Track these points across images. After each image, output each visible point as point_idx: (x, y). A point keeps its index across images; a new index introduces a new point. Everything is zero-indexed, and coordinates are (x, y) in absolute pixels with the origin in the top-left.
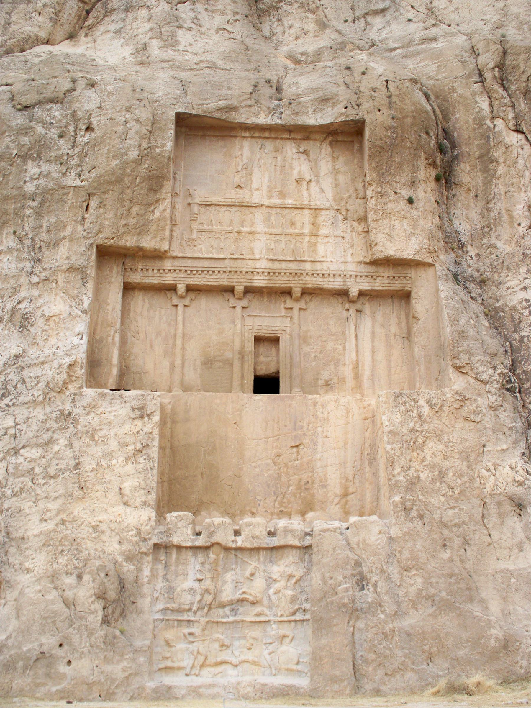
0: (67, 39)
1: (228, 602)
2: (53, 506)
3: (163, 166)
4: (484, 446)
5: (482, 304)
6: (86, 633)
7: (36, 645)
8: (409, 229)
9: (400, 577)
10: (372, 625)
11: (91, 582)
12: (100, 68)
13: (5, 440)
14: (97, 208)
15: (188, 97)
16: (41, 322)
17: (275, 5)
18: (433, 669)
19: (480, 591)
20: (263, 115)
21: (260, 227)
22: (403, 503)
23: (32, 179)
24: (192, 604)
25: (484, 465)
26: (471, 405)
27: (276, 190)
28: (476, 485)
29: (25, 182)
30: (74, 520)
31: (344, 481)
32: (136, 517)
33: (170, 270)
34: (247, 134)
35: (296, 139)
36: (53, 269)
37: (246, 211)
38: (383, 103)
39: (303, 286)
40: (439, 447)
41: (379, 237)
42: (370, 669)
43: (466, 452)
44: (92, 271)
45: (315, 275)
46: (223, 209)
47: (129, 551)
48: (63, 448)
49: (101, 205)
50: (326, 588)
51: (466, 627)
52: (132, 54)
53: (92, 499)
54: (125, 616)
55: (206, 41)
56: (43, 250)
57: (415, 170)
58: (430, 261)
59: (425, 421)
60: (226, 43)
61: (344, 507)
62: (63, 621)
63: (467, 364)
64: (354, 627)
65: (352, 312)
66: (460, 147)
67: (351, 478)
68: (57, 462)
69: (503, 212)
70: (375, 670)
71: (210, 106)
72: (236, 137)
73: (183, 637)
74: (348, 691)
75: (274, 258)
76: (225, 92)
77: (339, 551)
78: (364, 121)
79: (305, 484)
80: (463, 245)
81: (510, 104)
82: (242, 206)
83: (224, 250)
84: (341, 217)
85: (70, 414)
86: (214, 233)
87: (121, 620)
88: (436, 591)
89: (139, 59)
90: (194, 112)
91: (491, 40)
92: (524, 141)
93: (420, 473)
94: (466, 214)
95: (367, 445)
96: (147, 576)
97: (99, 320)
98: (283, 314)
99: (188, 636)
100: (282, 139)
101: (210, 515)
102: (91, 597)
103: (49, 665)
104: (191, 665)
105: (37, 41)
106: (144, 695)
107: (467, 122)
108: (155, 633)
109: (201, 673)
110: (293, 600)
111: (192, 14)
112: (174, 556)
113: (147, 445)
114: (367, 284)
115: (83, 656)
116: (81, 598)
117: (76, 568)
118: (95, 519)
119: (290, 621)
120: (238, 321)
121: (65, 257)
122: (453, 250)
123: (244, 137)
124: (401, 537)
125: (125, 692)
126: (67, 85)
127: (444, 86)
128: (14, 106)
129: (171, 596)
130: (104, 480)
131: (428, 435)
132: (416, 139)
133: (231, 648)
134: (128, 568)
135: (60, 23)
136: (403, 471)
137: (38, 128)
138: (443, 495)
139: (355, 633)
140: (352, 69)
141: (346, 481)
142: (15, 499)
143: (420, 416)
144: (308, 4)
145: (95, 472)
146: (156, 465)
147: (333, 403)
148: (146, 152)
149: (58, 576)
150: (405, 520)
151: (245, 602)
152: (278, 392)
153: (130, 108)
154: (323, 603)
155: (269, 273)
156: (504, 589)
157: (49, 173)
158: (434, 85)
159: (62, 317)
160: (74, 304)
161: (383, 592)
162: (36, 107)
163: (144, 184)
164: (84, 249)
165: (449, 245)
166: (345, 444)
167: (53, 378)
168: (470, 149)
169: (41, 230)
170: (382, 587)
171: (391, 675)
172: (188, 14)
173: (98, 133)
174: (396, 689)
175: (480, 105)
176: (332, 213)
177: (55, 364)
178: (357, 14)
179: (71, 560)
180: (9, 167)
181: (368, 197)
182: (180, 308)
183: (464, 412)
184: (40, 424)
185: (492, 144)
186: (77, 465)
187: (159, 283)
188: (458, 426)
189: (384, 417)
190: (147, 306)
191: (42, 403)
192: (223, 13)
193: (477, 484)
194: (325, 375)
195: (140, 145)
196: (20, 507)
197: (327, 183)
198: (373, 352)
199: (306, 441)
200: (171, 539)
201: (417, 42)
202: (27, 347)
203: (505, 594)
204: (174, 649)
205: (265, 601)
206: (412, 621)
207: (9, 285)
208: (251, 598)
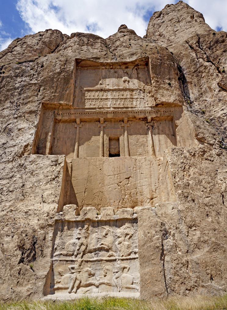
2: (8, 204)
3: (70, 74)
6: (9, 268)
24: (74, 251)
29: (16, 84)
32: (48, 207)
33: (73, 114)
34: (104, 68)
38: (155, 52)
41: (159, 96)
42: (177, 286)
48: (18, 179)
56: (20, 106)
67: (154, 190)
68: (14, 185)
73: (68, 270)
77: (152, 219)
79: (133, 194)
84: (142, 92)
85: (23, 164)
92: (211, 64)
93: (189, 181)
96: (51, 237)
115: (4, 282)
116: (10, 248)
118: (27, 209)
119: (127, 259)
129: (63, 247)
131: (190, 165)
145: (31, 189)
146: (61, 185)
149: (2, 237)
150: (186, 202)
154: (145, 247)
157: (25, 80)
164: (37, 104)
166: (151, 176)
169: (21, 99)
177: (20, 146)
179: (10, 229)
182: (78, 128)
183: (205, 156)
191: (12, 161)
192: (97, 49)
195: (61, 68)
198: (159, 141)
200: (65, 218)
204: (63, 277)
205: (114, 248)
206: (198, 256)
208: (106, 247)
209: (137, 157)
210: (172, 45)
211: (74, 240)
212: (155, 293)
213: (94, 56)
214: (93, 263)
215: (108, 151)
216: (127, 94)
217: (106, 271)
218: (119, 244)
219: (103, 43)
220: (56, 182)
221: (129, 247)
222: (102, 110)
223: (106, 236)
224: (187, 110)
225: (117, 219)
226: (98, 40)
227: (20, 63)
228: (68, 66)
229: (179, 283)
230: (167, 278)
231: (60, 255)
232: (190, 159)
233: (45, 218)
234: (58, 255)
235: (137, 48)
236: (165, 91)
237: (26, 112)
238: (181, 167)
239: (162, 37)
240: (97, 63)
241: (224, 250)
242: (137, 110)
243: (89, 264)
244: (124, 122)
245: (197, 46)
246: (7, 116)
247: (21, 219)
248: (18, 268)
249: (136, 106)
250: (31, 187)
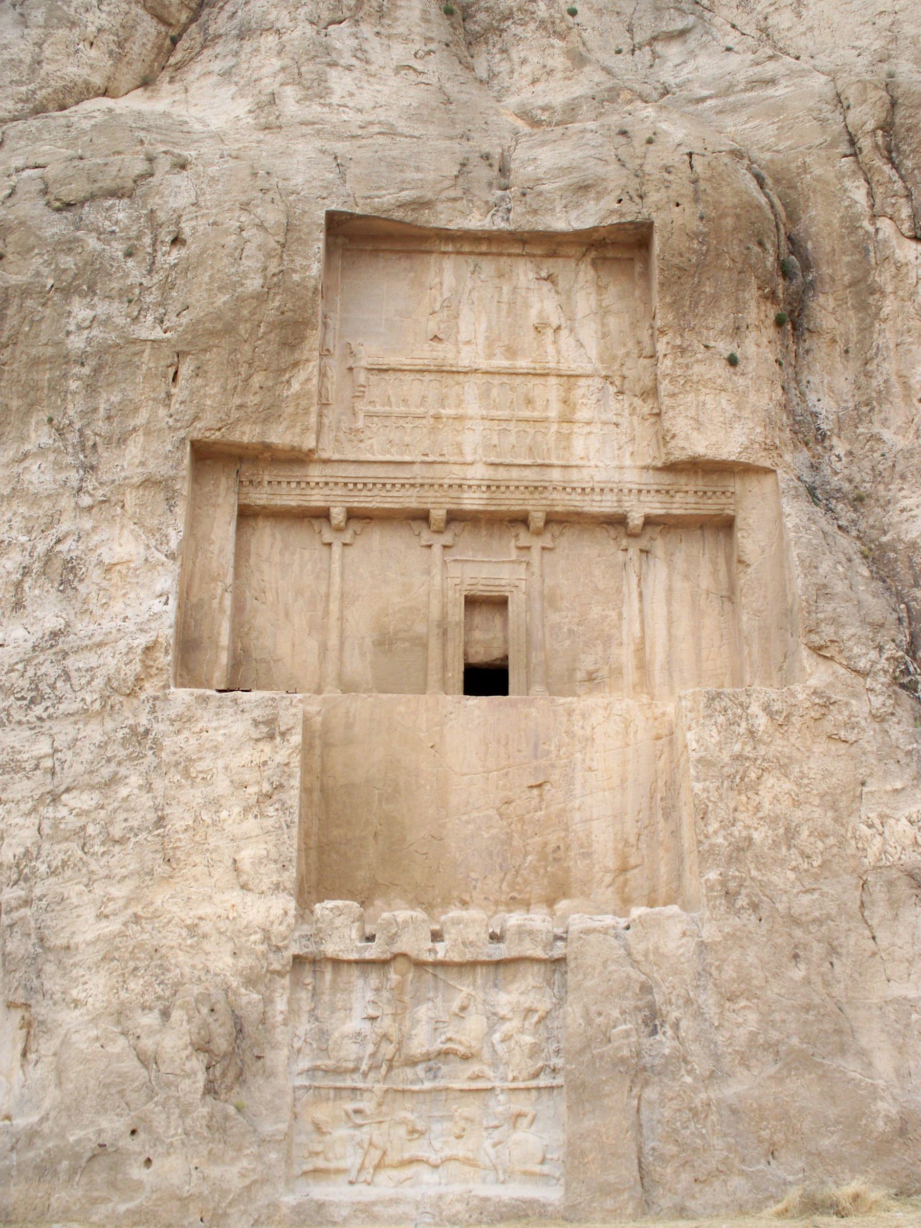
0: (138, 87)
1: (422, 1055)
2: (119, 891)
4: (863, 784)
5: (858, 538)
6: (177, 1111)
7: (91, 1132)
8: (730, 410)
9: (718, 1011)
10: (670, 1094)
11: (185, 1023)
12: (195, 137)
13: (35, 779)
15: (348, 185)
16: (96, 574)
17: (496, 24)
18: (777, 1170)
19: (857, 1036)
20: (476, 214)
21: (473, 408)
22: (723, 883)
23: (79, 328)
24: (360, 1059)
25: (864, 817)
26: (840, 712)
27: (501, 344)
28: (849, 852)
29: (68, 333)
30: (155, 916)
31: (620, 846)
33: (317, 483)
34: (450, 248)
35: (534, 256)
37: (450, 380)
38: (684, 191)
39: (548, 509)
40: (784, 786)
41: (679, 423)
43: (832, 795)
44: (184, 487)
45: (568, 490)
46: (409, 377)
47: (251, 968)
48: (136, 791)
49: (199, 372)
50: (591, 1032)
51: (833, 1097)
52: (250, 112)
54: (244, 1081)
55: (378, 87)
56: (100, 450)
57: (739, 307)
58: (767, 464)
59: (760, 741)
60: (413, 92)
61: (621, 891)
62: (136, 1090)
63: (832, 641)
64: (639, 1099)
65: (633, 553)
66: (818, 266)
67: (632, 840)
68: (125, 815)
69: (894, 379)
70: (676, 1173)
71: (385, 199)
72: (430, 252)
74: (629, 1211)
75: (498, 461)
76: (410, 175)
77: (613, 967)
78: (653, 223)
79: (554, 851)
80: (824, 436)
81: (903, 192)
82: (442, 372)
83: (411, 448)
85: (147, 732)
86: (393, 419)
87: (237, 1089)
88: (781, 1036)
89: (263, 121)
90: (358, 211)
91: (870, 82)
93: (752, 831)
94: (829, 383)
95: (660, 784)
96: (282, 1012)
97: (197, 570)
98: (514, 558)
100: (509, 255)
101: (390, 905)
102: (186, 1048)
103: (115, 1167)
104: (358, 1166)
105: (87, 92)
106: (277, 1218)
107: (828, 224)
108: (297, 1110)
109: (376, 1179)
110: (535, 1051)
111: (354, 43)
112: (328, 976)
113: (281, 786)
114: (658, 505)
115: (172, 1150)
116: (169, 1050)
117: (159, 998)
118: (191, 914)
119: (528, 1089)
120: (436, 571)
121: (137, 461)
122: (807, 444)
123: (444, 253)
124: (720, 942)
125: (245, 1212)
126: (140, 167)
127: (789, 163)
128: (48, 204)
129: (324, 1046)
130: (206, 846)
131: (766, 765)
132: (742, 253)
133: (427, 1136)
134: (250, 997)
135: (126, 59)
136: (723, 827)
137: (90, 241)
138: (793, 869)
139: (642, 1109)
140: (630, 134)
141: (625, 846)
142: (53, 880)
143: (751, 733)
144: (553, 23)
146: (296, 820)
147: (601, 711)
148: (275, 279)
150: (728, 913)
151: (451, 1057)
152: (505, 693)
153: (248, 204)
154: (587, 1057)
155: (489, 487)
156: (899, 1031)
157: (109, 318)
158: (772, 161)
159: (132, 565)
160: (153, 543)
161: (690, 1037)
162: (87, 204)
163: (273, 335)
164: (169, 447)
165: (800, 436)
166: (623, 780)
167: (118, 671)
168: (835, 271)
169: (95, 416)
170: (688, 1028)
171: (704, 1182)
172: (347, 42)
173: (193, 248)
174: (714, 1206)
175: (851, 194)
176: (597, 382)
177: (122, 646)
178: (638, 39)
179: (151, 984)
180: (40, 308)
181: (660, 355)
182: (337, 549)
183: (828, 726)
184: (96, 751)
185: (873, 261)
186: (160, 821)
187: (299, 506)
188: (817, 749)
189: (690, 736)
190: (279, 544)
191: (99, 713)
192: (406, 40)
193: (851, 850)
194: (588, 662)
195: (265, 269)
196: (62, 894)
197: (588, 332)
199: (555, 776)
200: (322, 948)
201: (742, 87)
202: (72, 617)
203: (901, 1041)
204: (328, 1137)
205: (486, 1054)
207: (41, 512)
208: (462, 1050)
211: (355, 1024)
241: (820, 1072)
246: (49, 497)
250: (188, 826)
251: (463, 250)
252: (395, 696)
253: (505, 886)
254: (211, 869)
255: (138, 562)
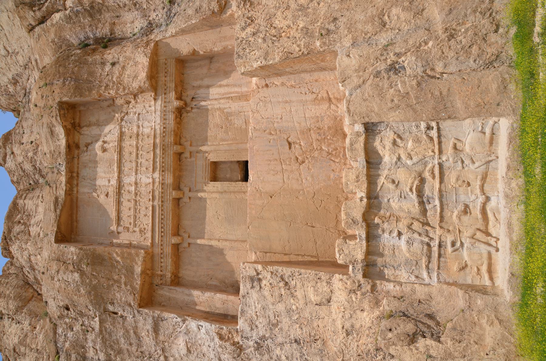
3: (86, 254)
10: (440, 53)
11: (397, 348)
14: (114, 306)
24: (422, 242)
29: (99, 359)
32: (339, 293)
33: (162, 249)
34: (75, 189)
36: (155, 343)
38: (49, 89)
40: (279, 15)
41: (135, 85)
42: (489, 50)
44: (157, 313)
48: (283, 352)
50: (403, 105)
53: (325, 331)
56: (143, 350)
57: (95, 63)
59: (258, 30)
67: (314, 96)
72: (77, 198)
77: (366, 95)
79: (320, 135)
85: (256, 342)
96: (394, 286)
99: (455, 248)
100: (78, 164)
114: (171, 94)
117: (384, 358)
118: (340, 333)
119: (440, 143)
123: (77, 192)
129: (414, 263)
130: (309, 318)
131: (269, 25)
133: (468, 203)
134: (386, 305)
138: (319, 4)
145: (303, 326)
146: (297, 270)
147: (255, 115)
150: (337, 33)
153: (52, 277)
154: (418, 107)
155: (163, 171)
157: (92, 341)
163: (97, 268)
164: (141, 318)
166: (286, 102)
167: (230, 353)
169: (130, 350)
177: (220, 350)
182: (191, 241)
187: (171, 258)
192: (37, 206)
195: (72, 271)
200: (360, 261)
204: (469, 263)
205: (419, 168)
206: (436, 12)
208: (416, 182)
209: (250, 128)
210: (36, 61)
212: (502, 88)
213: (52, 208)
214: (445, 207)
215: (237, 183)
216: (129, 144)
217: (460, 182)
218: (411, 159)
219: (25, 195)
220: (293, 279)
221: (418, 139)
222: (157, 193)
223: (397, 183)
224: (164, 32)
225: (365, 163)
226: (19, 205)
227: (58, 353)
228: (70, 256)
229: (484, 46)
230: (474, 66)
231: (428, 269)
232: (257, 25)
233: (359, 298)
234: (429, 273)
235: (41, 124)
236: (127, 73)
237: (156, 338)
238: (273, 43)
239: (20, 81)
240: (65, 202)
242: (161, 126)
243: (447, 214)
244: (182, 153)
245: (39, 9)
247: (360, 342)
248: (450, 343)
249: (152, 129)
251: (76, 184)
252: (248, 215)
253: (337, 160)
254: (320, 317)
255: (187, 338)
